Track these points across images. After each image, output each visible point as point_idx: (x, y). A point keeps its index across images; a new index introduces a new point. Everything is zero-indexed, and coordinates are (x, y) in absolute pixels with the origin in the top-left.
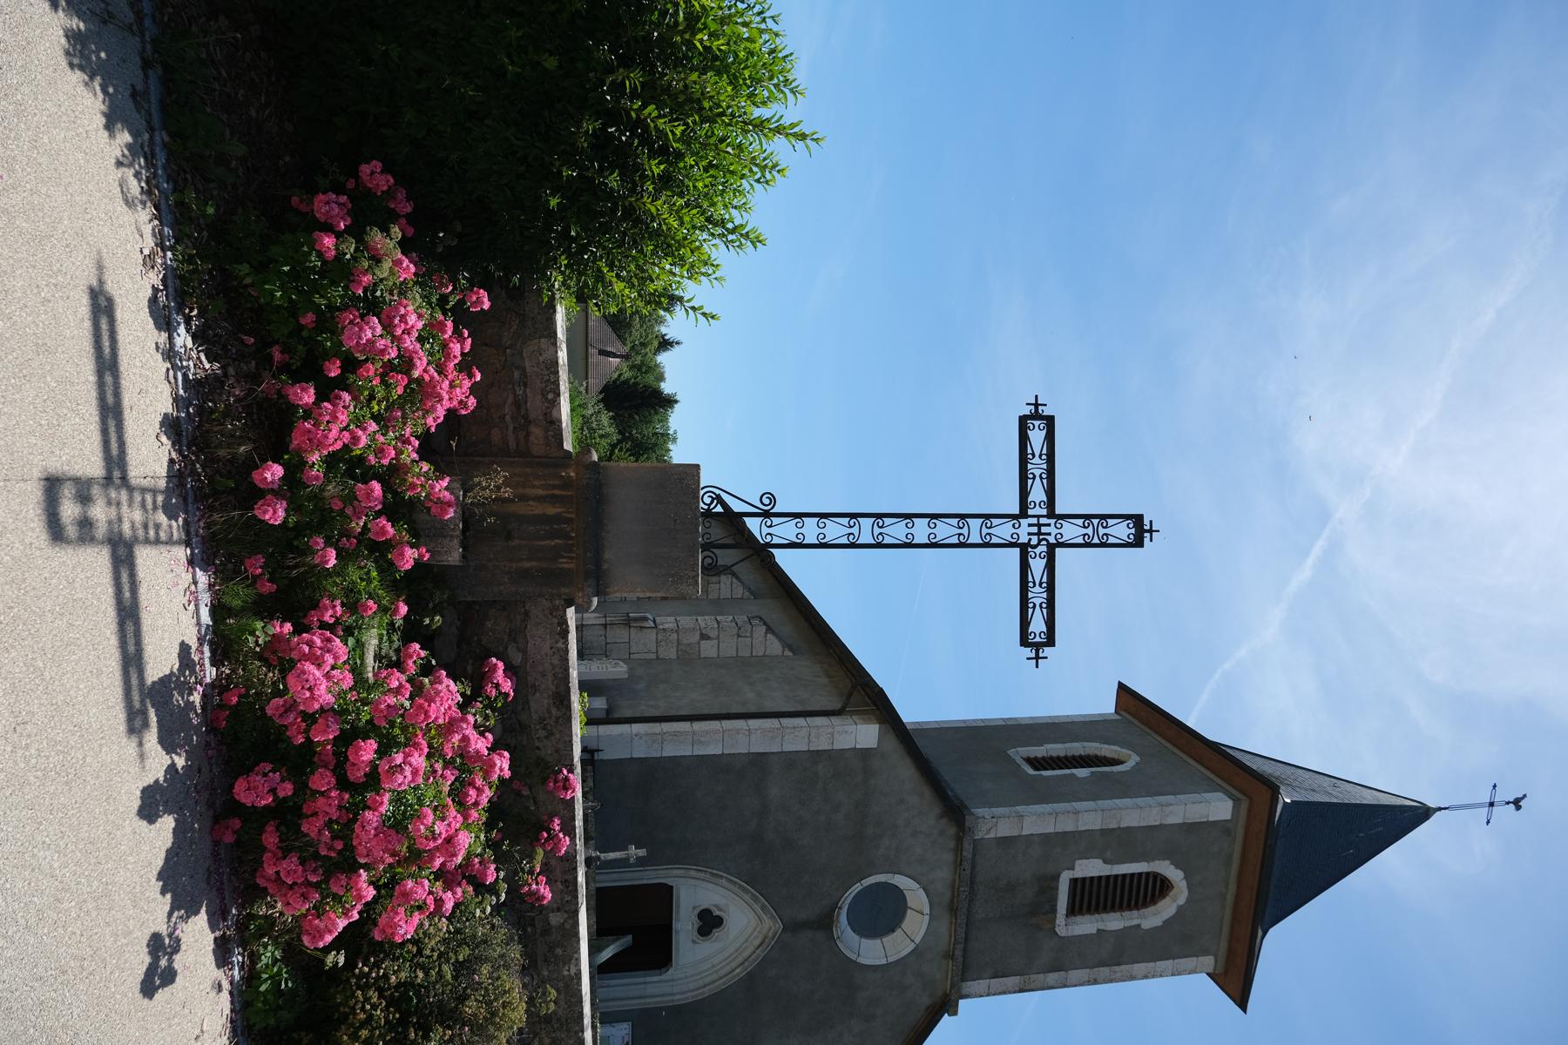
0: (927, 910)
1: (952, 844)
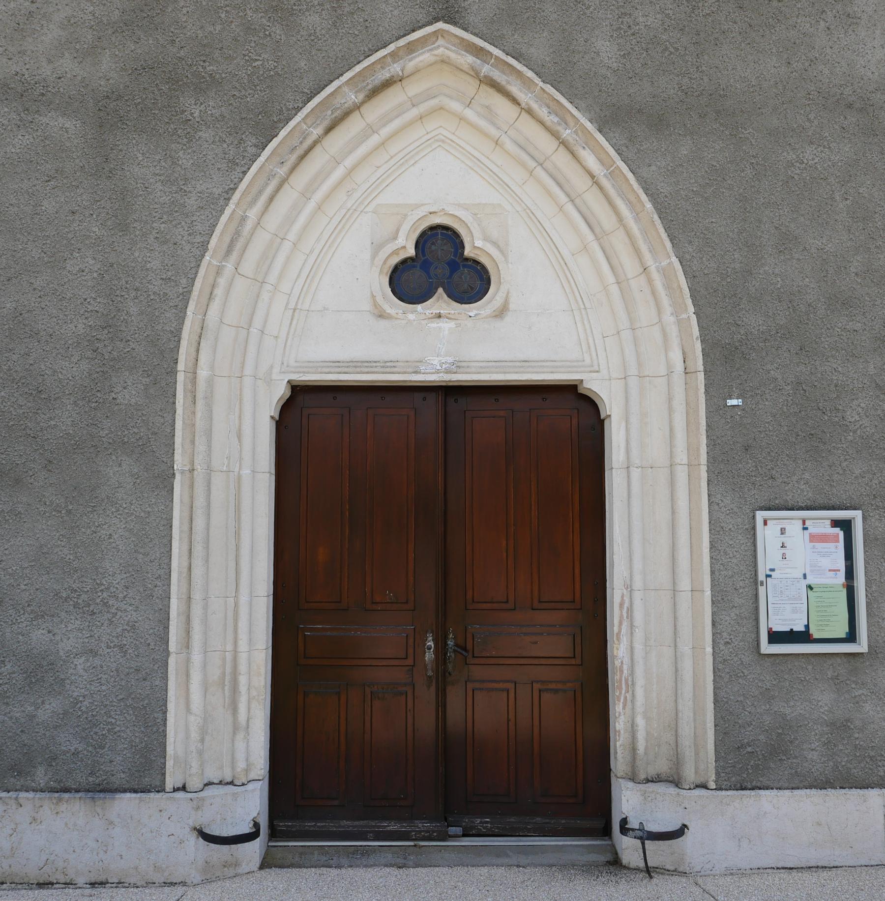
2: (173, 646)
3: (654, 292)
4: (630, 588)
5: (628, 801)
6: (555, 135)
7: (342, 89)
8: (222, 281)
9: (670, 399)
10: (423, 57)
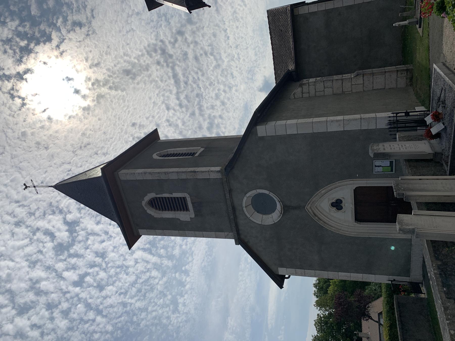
1: (241, 232)
10: (310, 210)
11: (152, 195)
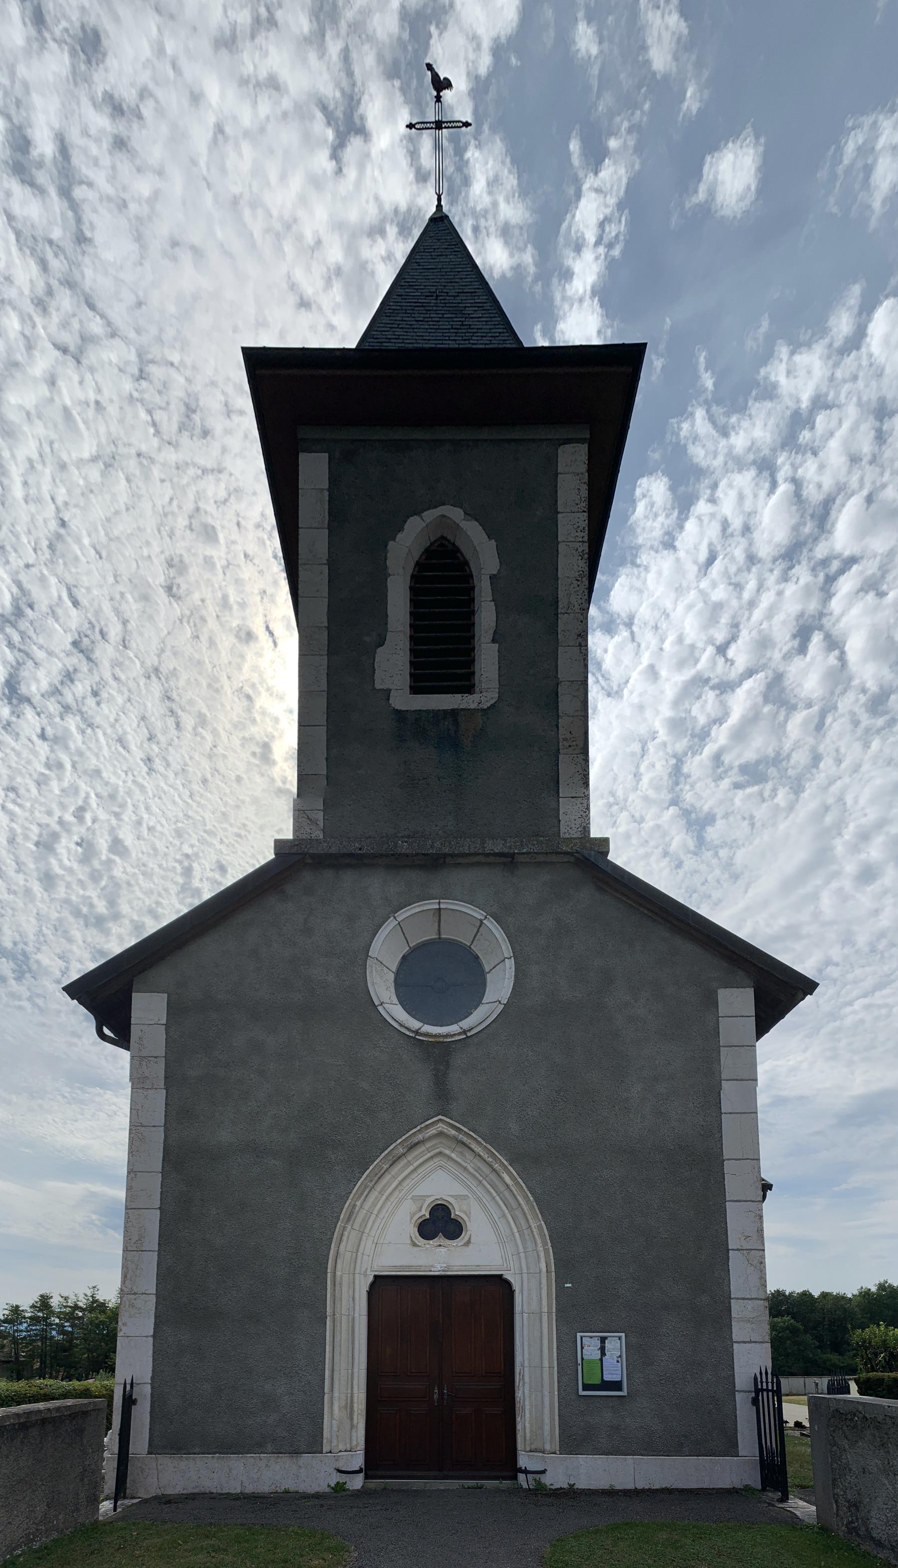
0: (433, 905)
1: (329, 874)
2: (326, 1390)
3: (534, 1236)
4: (523, 1366)
5: (523, 1461)
6: (491, 1166)
7: (396, 1148)
8: (346, 1233)
9: (540, 1283)
10: (432, 1131)
11: (484, 556)
